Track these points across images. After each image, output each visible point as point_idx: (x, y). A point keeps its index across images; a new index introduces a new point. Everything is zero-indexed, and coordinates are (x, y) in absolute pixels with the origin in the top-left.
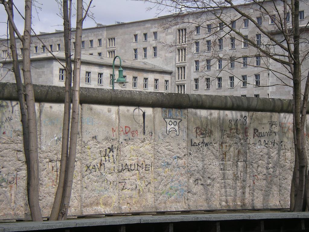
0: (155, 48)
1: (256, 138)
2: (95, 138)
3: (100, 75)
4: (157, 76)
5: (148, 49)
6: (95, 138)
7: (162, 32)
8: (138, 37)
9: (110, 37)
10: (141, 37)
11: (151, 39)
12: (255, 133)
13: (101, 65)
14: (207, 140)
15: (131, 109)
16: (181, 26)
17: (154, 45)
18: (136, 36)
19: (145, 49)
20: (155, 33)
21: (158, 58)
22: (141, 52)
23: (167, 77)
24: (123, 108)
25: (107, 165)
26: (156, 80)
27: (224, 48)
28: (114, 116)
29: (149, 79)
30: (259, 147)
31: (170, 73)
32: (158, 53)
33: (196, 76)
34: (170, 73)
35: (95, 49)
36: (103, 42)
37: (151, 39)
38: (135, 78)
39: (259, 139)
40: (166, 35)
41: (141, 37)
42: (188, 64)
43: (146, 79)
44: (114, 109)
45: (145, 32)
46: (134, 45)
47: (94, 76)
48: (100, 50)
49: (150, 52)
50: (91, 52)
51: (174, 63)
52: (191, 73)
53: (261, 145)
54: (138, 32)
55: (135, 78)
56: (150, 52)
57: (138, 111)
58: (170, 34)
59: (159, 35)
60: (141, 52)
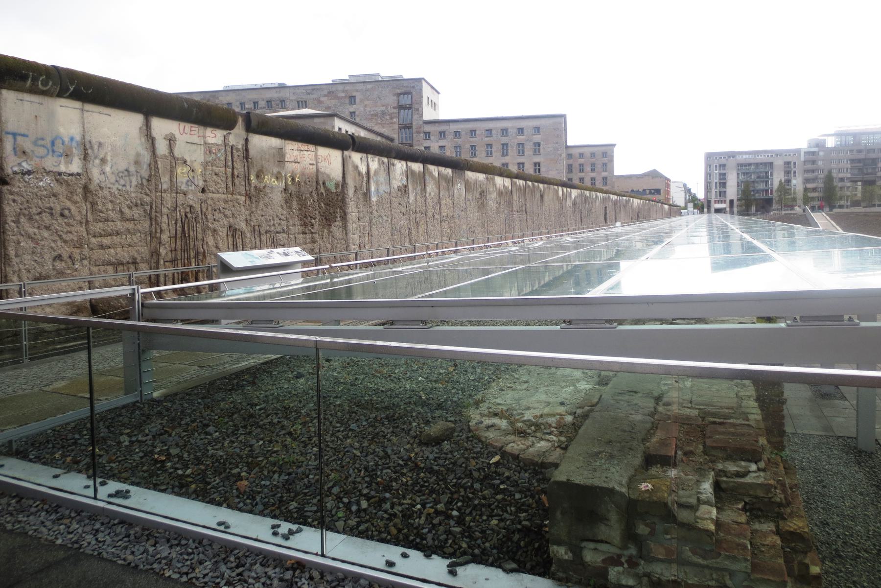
28: (437, 175)
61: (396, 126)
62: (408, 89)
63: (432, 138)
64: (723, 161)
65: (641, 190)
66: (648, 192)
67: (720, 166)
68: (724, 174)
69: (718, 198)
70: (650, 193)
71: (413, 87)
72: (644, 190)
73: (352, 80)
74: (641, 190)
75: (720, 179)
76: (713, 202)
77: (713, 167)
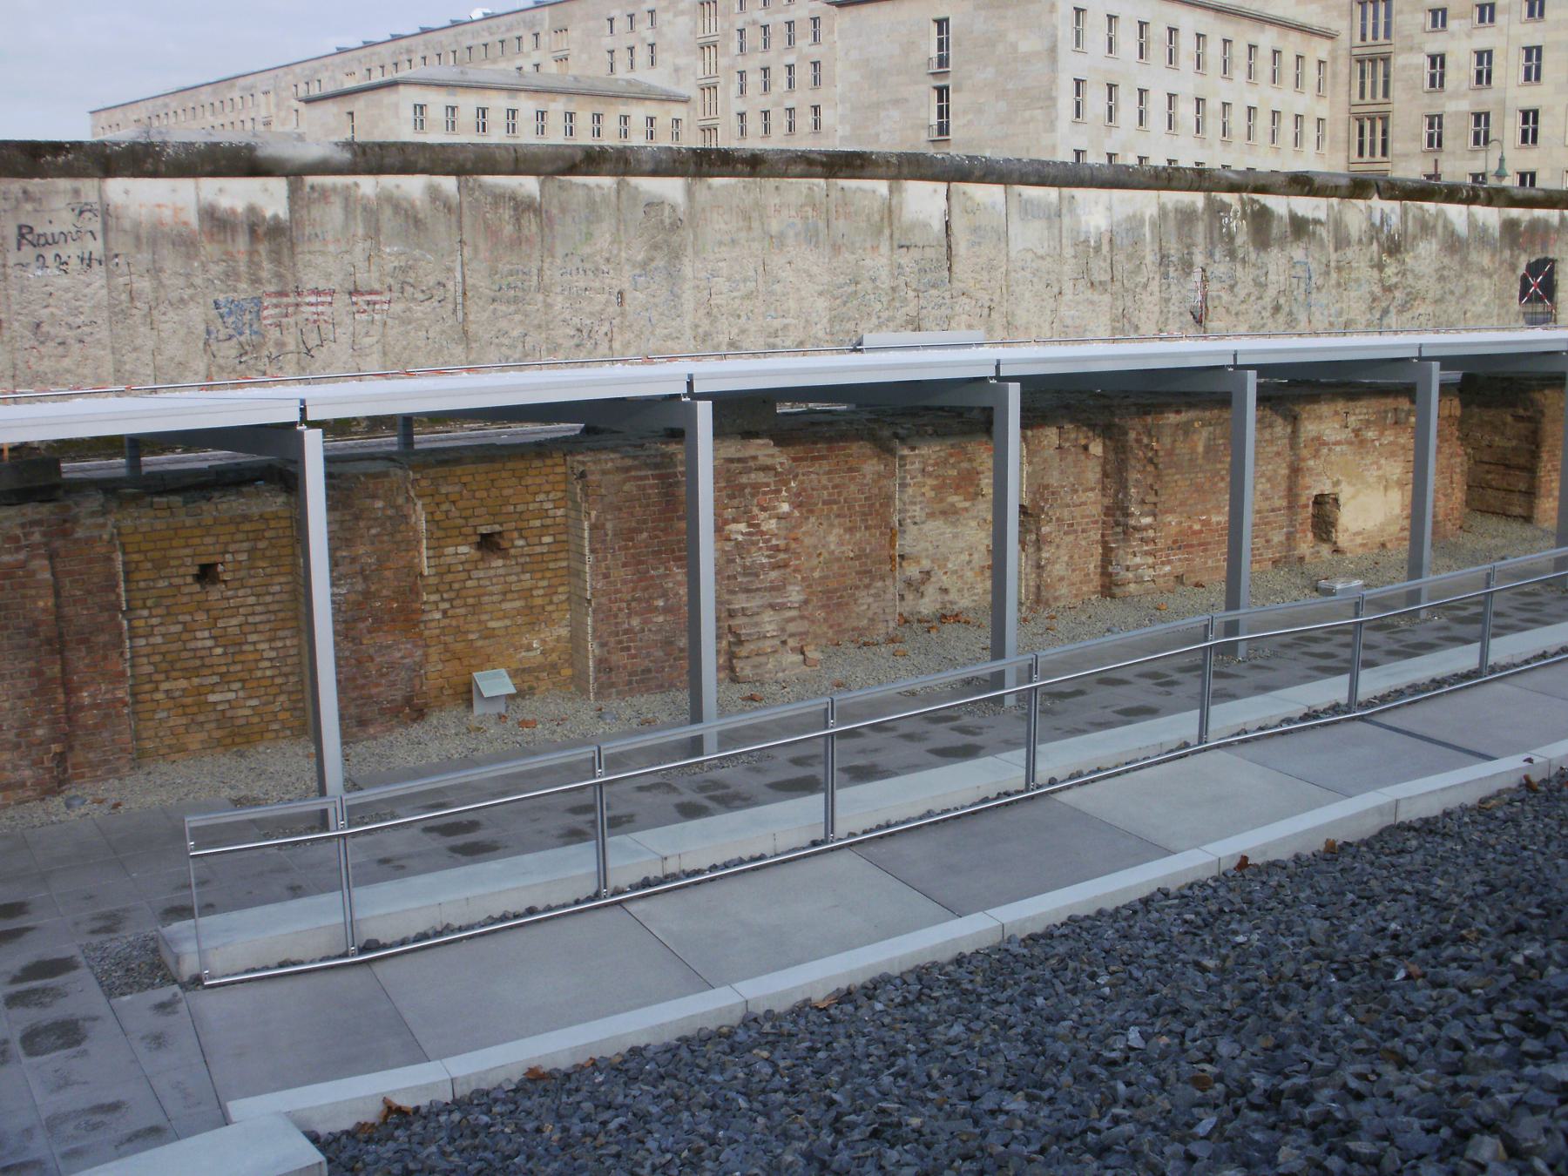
1: (27, 248)
3: (513, 113)
4: (652, 109)
5: (637, 50)
7: (666, 10)
8: (616, 24)
10: (621, 24)
11: (643, 28)
12: (22, 236)
13: (513, 90)
17: (651, 41)
18: (611, 20)
19: (631, 49)
21: (658, 69)
22: (622, 58)
23: (678, 111)
26: (651, 120)
27: (798, 43)
29: (633, 118)
30: (39, 273)
31: (686, 101)
32: (659, 57)
33: (739, 106)
34: (686, 101)
35: (528, 55)
36: (544, 39)
37: (643, 28)
38: (598, 117)
39: (38, 251)
40: (675, 15)
41: (621, 24)
42: (722, 80)
43: (625, 119)
45: (630, 11)
46: (608, 42)
47: (497, 118)
48: (536, 57)
49: (642, 55)
50: (518, 63)
51: (693, 79)
52: (730, 101)
53: (44, 266)
54: (615, 13)
55: (598, 117)
58: (683, 13)
59: (661, 17)
60: (622, 58)
63: (1452, 24)
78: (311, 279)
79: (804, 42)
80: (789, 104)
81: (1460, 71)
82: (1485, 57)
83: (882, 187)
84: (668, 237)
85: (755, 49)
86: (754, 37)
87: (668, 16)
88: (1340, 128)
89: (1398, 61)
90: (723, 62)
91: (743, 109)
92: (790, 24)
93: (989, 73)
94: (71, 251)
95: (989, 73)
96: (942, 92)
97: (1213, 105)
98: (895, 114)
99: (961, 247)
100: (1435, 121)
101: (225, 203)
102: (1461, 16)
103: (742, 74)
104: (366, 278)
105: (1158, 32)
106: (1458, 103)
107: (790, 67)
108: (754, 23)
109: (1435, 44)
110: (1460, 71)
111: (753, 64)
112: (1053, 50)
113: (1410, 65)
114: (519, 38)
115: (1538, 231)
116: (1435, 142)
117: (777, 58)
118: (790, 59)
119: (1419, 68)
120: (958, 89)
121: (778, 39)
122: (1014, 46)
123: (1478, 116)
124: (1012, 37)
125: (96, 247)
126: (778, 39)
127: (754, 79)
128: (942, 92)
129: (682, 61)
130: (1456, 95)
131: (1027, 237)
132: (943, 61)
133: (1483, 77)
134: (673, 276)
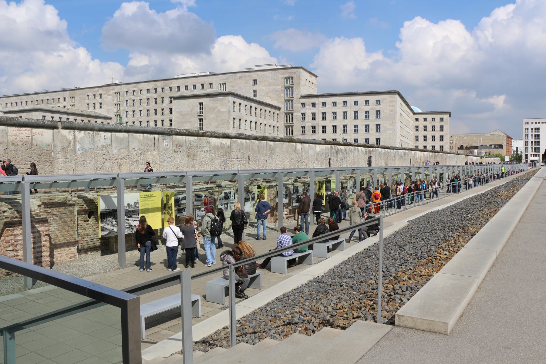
0: (100, 103)
2: (134, 148)
6: (134, 148)
7: (105, 94)
9: (71, 96)
10: (91, 97)
11: (98, 98)
14: (181, 150)
15: (149, 135)
16: (116, 91)
18: (88, 96)
19: (94, 104)
20: (101, 94)
21: (103, 109)
22: (91, 106)
24: (145, 135)
25: (140, 161)
32: (103, 106)
36: (67, 99)
37: (98, 98)
41: (91, 97)
44: (142, 135)
46: (87, 101)
48: (64, 104)
49: (98, 105)
50: (59, 105)
56: (98, 105)
57: (152, 136)
58: (110, 95)
59: (103, 96)
60: (91, 106)
61: (283, 99)
62: (291, 76)
64: (537, 126)
65: (488, 145)
66: (493, 146)
67: (536, 129)
68: (538, 135)
69: (534, 153)
70: (495, 147)
71: (295, 73)
72: (491, 145)
73: (257, 69)
74: (488, 145)
75: (535, 139)
76: (529, 156)
77: (530, 130)
78: (233, 156)
79: (145, 104)
80: (141, 120)
81: (309, 117)
82: (313, 114)
83: (294, 144)
84: (272, 150)
85: (131, 106)
86: (131, 103)
87: (106, 96)
88: (282, 129)
89: (295, 114)
90: (121, 108)
91: (127, 121)
92: (141, 100)
93: (213, 116)
94: (205, 149)
95: (213, 116)
96: (201, 120)
97: (258, 123)
98: (189, 125)
99: (303, 154)
100: (304, 127)
101: (223, 142)
102: (308, 105)
103: (127, 112)
104: (239, 156)
105: (248, 107)
106: (308, 124)
107: (141, 111)
108: (131, 99)
109: (303, 111)
110: (309, 117)
111: (130, 109)
112: (229, 111)
113: (297, 115)
114: (59, 99)
115: (370, 151)
116: (303, 132)
117: (137, 108)
118: (141, 109)
119: (299, 116)
120: (205, 119)
121: (137, 103)
122: (219, 110)
123: (313, 127)
124: (219, 108)
125: (208, 149)
126: (137, 103)
127: (131, 113)
128: (201, 120)
129: (109, 108)
130: (308, 122)
131: (311, 152)
132: (201, 112)
133: (314, 119)
134: (272, 158)
